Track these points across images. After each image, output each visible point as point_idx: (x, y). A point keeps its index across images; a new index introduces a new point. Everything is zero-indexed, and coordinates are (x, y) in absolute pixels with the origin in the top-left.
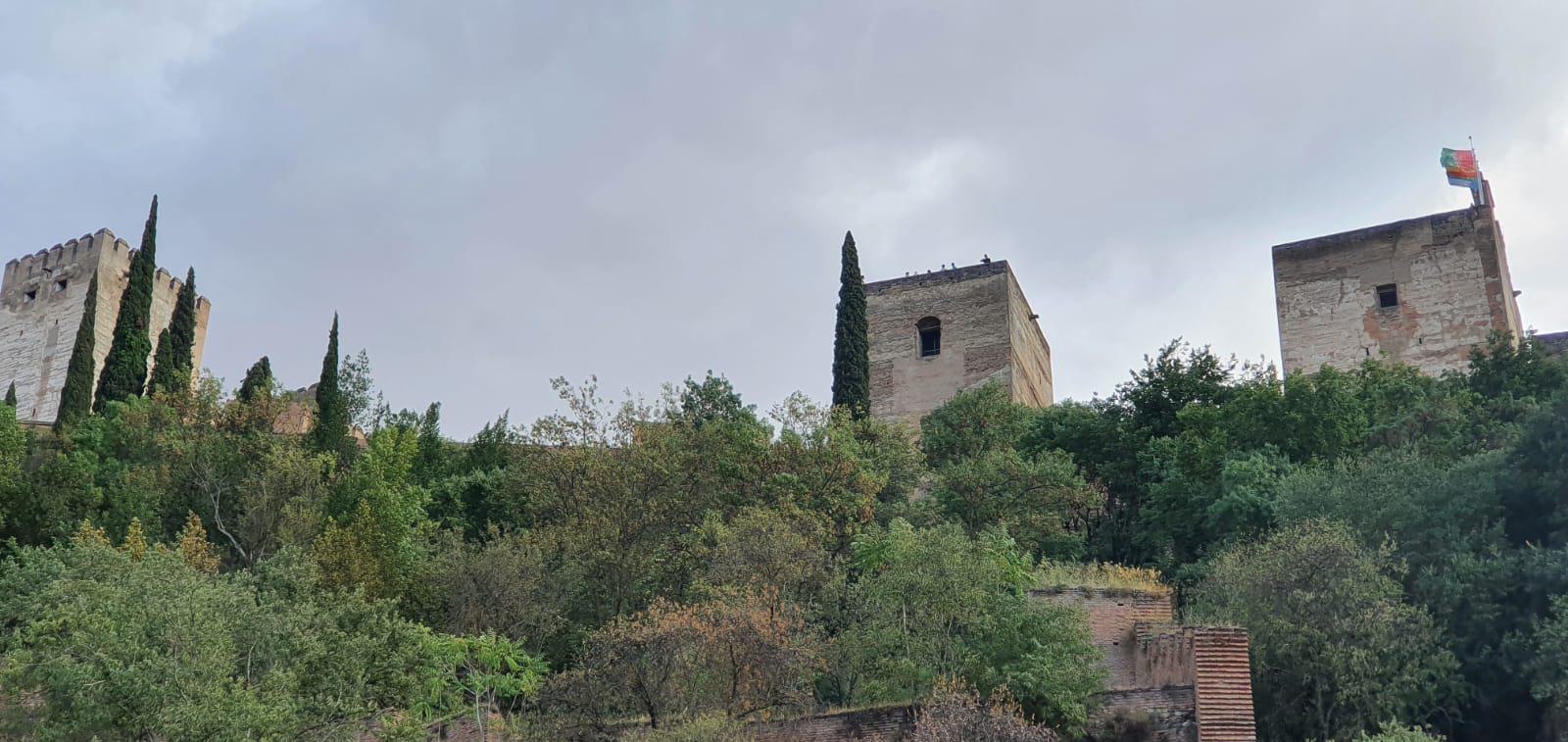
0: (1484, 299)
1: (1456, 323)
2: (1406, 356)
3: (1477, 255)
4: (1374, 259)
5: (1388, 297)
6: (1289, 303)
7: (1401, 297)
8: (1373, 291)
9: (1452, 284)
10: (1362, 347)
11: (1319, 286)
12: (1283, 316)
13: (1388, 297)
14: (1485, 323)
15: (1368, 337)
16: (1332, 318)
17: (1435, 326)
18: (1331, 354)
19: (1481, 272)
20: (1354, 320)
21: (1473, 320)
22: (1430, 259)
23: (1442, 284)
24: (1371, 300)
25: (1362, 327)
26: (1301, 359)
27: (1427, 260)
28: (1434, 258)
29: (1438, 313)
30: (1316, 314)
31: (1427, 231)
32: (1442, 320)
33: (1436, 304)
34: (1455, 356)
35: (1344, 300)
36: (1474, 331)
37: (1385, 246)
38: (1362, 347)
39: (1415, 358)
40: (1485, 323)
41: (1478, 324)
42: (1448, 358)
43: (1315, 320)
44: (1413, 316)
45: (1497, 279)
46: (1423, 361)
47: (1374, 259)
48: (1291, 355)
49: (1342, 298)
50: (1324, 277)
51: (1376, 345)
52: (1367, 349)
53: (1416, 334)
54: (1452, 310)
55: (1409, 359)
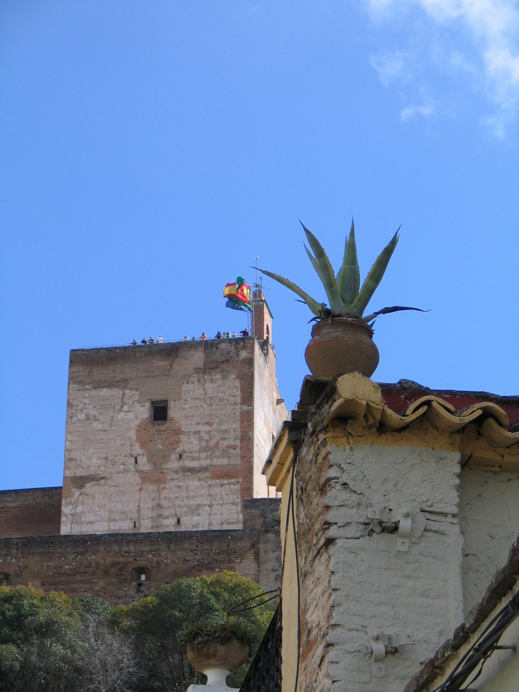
0: (237, 425)
1: (212, 443)
2: (167, 469)
3: (237, 383)
4: (152, 374)
5: (160, 412)
6: (78, 406)
7: (172, 413)
8: (148, 405)
9: (214, 407)
10: (132, 455)
11: (104, 392)
12: (71, 418)
13: (160, 412)
14: (234, 448)
15: (138, 447)
16: (111, 425)
17: (194, 444)
18: (106, 458)
19: (238, 399)
20: (129, 429)
21: (226, 443)
22: (199, 381)
23: (205, 406)
25: (134, 438)
26: (81, 460)
27: (196, 382)
28: (202, 380)
29: (198, 432)
30: (99, 420)
32: (201, 440)
33: (198, 424)
34: (207, 474)
35: (125, 408)
36: (225, 453)
37: (164, 363)
38: (132, 455)
39: (174, 472)
40: (234, 448)
41: (229, 447)
42: (201, 475)
44: (178, 432)
45: (250, 408)
46: (180, 475)
47: (152, 374)
48: (73, 455)
49: (122, 407)
50: (111, 384)
51: (143, 455)
52: (136, 458)
53: (178, 450)
54: (210, 431)
55: (169, 472)
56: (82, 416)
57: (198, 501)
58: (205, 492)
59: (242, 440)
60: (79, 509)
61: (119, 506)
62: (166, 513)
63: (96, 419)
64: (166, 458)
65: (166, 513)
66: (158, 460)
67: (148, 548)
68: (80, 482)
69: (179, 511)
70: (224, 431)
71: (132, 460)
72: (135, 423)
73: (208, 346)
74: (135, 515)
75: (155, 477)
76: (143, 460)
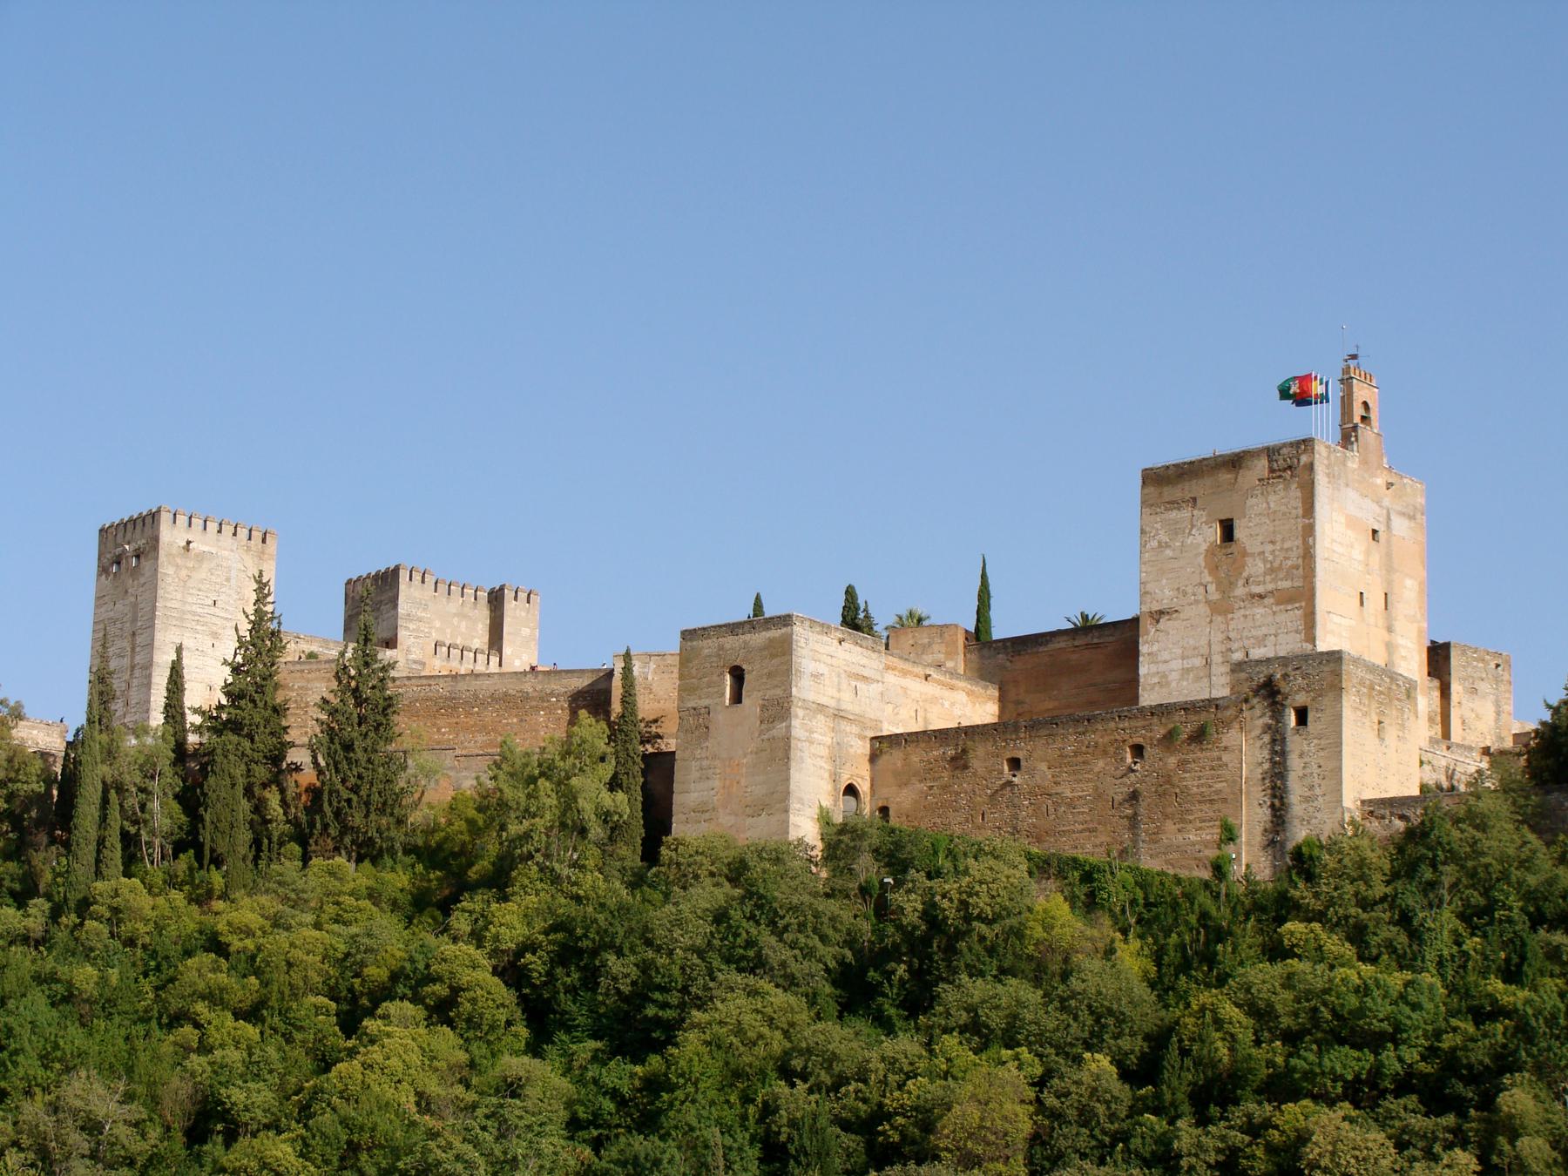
0: (1299, 542)
1: (1276, 565)
7: (1237, 534)
11: (1174, 514)
19: (1300, 511)
24: (1216, 532)
31: (1262, 465)
32: (1265, 561)
42: (1266, 601)
43: (1169, 552)
44: (1244, 554)
48: (1149, 587)
56: (1155, 544)
57: (1264, 630)
58: (1270, 619)
59: (1304, 558)
60: (1155, 648)
61: (1192, 642)
62: (1235, 646)
63: (1168, 546)
64: (1232, 584)
65: (1235, 646)
66: (1226, 586)
67: (1141, 723)
68: (1158, 615)
69: (1247, 643)
70: (1287, 550)
71: (1202, 589)
72: (1204, 547)
73: (1271, 452)
74: (1205, 651)
75: (1221, 609)
76: (1212, 588)
